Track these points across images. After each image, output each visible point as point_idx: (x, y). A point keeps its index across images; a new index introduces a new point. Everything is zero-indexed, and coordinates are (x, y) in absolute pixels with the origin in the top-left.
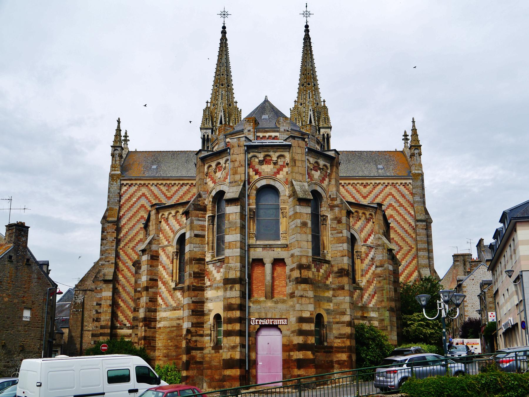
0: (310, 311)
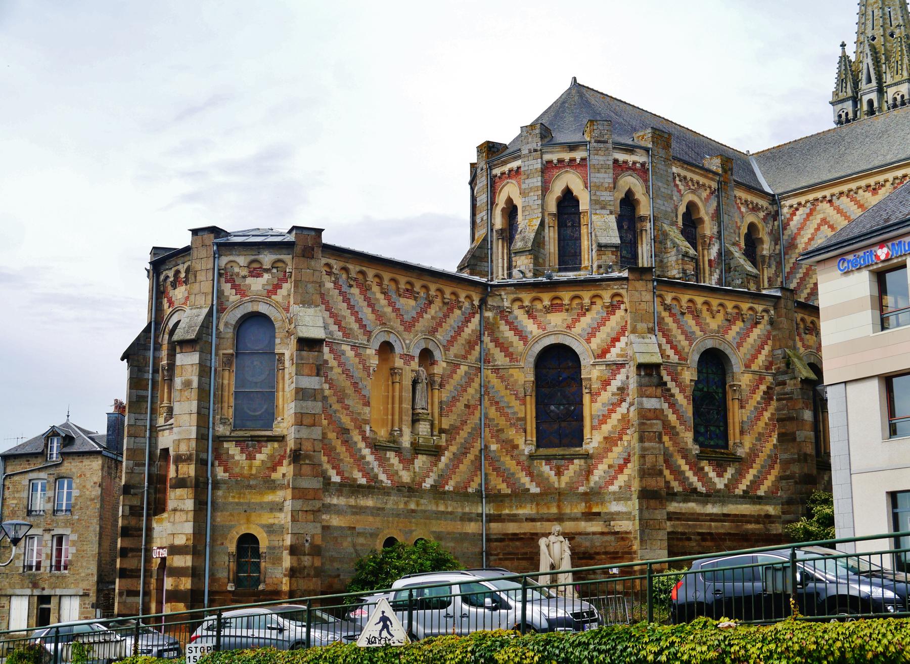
0: (186, 534)
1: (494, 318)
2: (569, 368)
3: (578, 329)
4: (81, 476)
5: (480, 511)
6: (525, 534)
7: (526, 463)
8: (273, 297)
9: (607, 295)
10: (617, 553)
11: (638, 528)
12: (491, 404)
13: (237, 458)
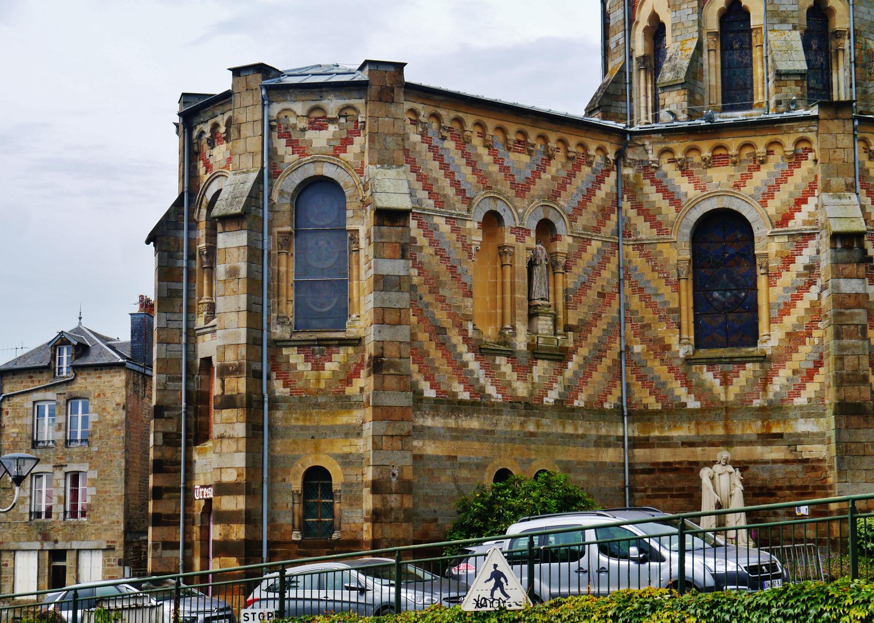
0: (237, 468)
1: (636, 176)
2: (737, 241)
3: (749, 188)
4: (99, 395)
5: (620, 433)
6: (681, 463)
7: (681, 370)
8: (342, 155)
9: (788, 142)
10: (807, 487)
11: (834, 454)
12: (634, 292)
13: (300, 368)
